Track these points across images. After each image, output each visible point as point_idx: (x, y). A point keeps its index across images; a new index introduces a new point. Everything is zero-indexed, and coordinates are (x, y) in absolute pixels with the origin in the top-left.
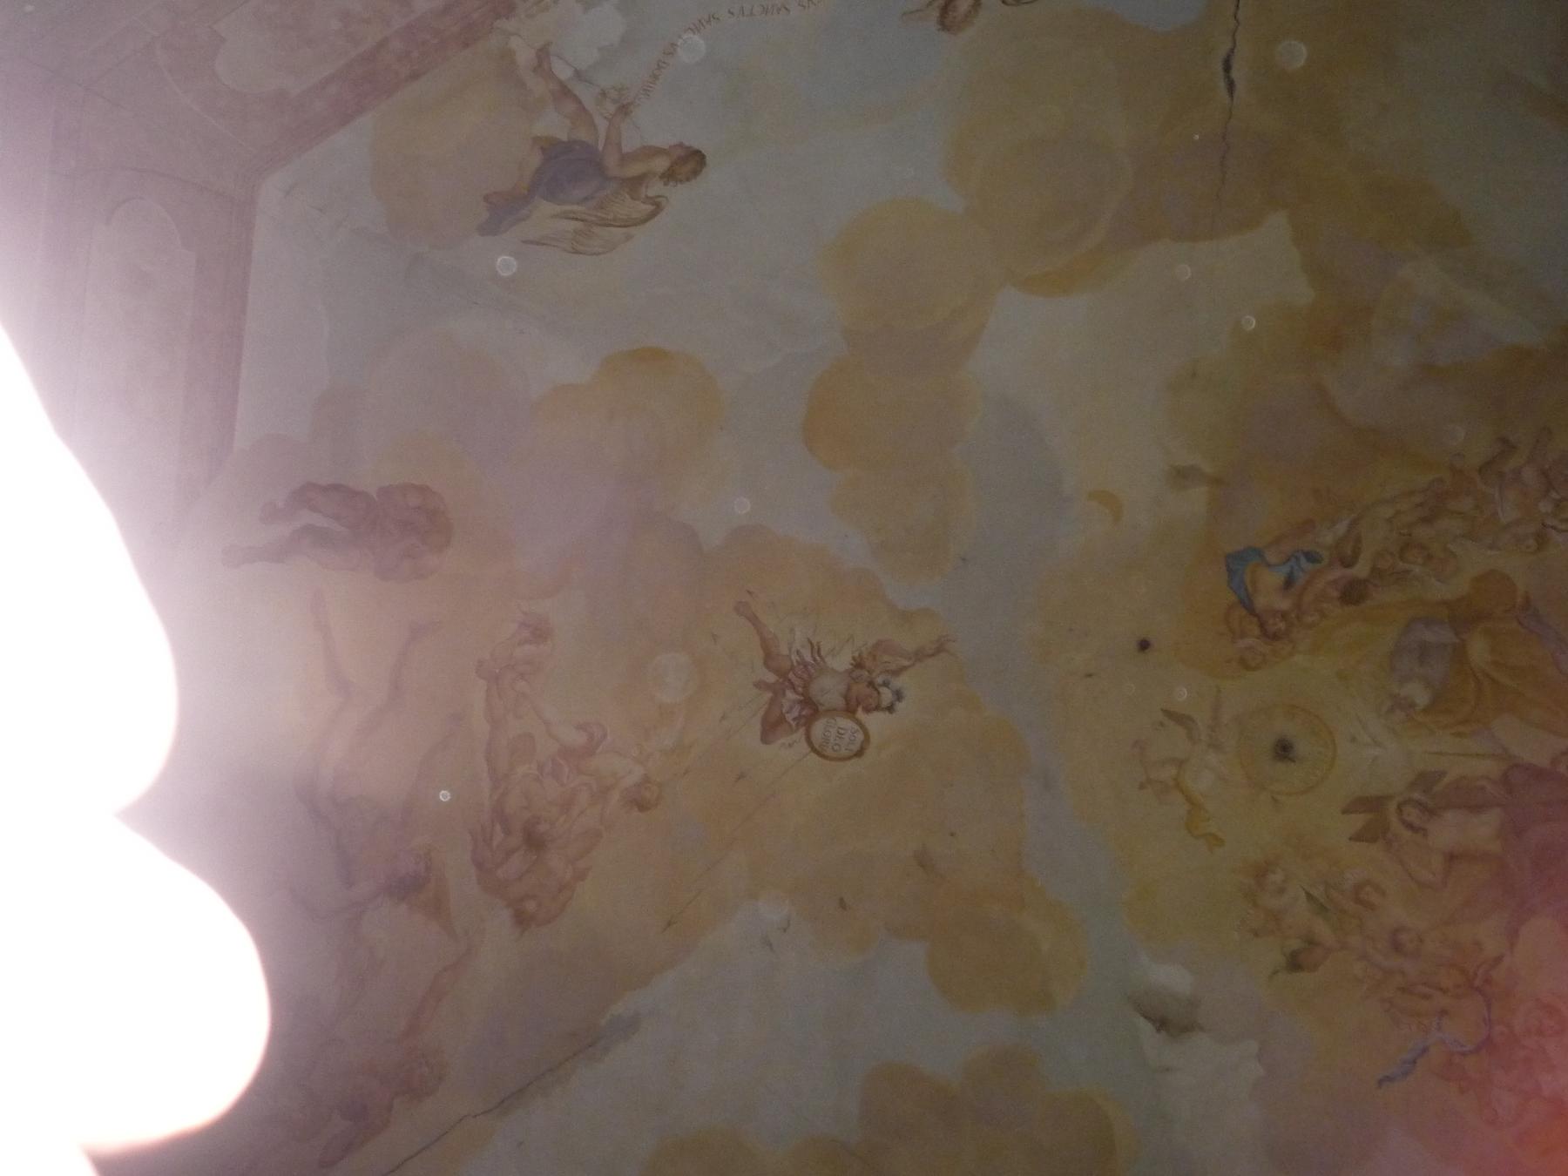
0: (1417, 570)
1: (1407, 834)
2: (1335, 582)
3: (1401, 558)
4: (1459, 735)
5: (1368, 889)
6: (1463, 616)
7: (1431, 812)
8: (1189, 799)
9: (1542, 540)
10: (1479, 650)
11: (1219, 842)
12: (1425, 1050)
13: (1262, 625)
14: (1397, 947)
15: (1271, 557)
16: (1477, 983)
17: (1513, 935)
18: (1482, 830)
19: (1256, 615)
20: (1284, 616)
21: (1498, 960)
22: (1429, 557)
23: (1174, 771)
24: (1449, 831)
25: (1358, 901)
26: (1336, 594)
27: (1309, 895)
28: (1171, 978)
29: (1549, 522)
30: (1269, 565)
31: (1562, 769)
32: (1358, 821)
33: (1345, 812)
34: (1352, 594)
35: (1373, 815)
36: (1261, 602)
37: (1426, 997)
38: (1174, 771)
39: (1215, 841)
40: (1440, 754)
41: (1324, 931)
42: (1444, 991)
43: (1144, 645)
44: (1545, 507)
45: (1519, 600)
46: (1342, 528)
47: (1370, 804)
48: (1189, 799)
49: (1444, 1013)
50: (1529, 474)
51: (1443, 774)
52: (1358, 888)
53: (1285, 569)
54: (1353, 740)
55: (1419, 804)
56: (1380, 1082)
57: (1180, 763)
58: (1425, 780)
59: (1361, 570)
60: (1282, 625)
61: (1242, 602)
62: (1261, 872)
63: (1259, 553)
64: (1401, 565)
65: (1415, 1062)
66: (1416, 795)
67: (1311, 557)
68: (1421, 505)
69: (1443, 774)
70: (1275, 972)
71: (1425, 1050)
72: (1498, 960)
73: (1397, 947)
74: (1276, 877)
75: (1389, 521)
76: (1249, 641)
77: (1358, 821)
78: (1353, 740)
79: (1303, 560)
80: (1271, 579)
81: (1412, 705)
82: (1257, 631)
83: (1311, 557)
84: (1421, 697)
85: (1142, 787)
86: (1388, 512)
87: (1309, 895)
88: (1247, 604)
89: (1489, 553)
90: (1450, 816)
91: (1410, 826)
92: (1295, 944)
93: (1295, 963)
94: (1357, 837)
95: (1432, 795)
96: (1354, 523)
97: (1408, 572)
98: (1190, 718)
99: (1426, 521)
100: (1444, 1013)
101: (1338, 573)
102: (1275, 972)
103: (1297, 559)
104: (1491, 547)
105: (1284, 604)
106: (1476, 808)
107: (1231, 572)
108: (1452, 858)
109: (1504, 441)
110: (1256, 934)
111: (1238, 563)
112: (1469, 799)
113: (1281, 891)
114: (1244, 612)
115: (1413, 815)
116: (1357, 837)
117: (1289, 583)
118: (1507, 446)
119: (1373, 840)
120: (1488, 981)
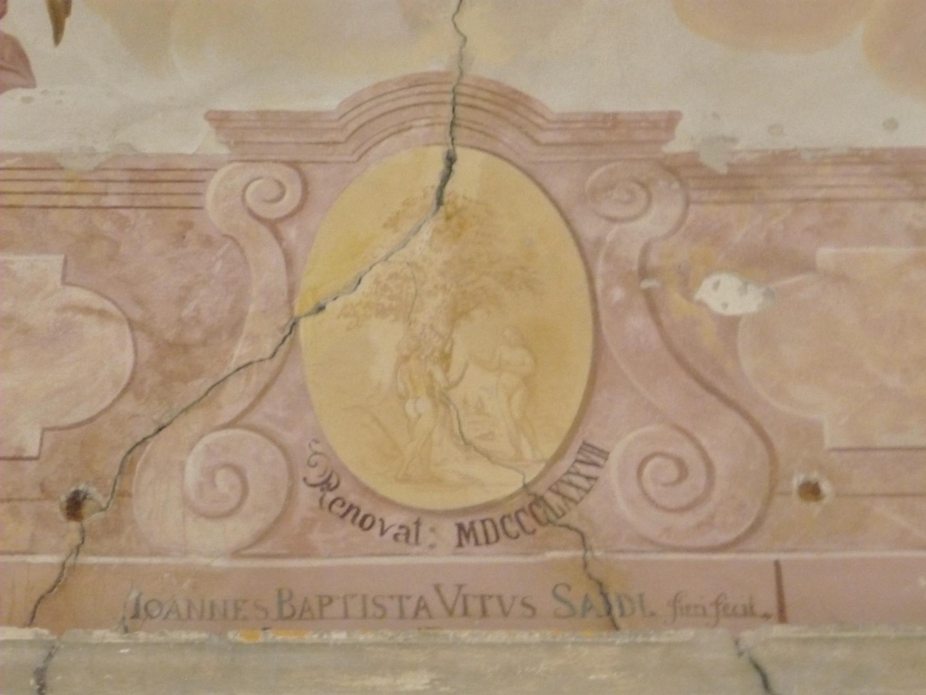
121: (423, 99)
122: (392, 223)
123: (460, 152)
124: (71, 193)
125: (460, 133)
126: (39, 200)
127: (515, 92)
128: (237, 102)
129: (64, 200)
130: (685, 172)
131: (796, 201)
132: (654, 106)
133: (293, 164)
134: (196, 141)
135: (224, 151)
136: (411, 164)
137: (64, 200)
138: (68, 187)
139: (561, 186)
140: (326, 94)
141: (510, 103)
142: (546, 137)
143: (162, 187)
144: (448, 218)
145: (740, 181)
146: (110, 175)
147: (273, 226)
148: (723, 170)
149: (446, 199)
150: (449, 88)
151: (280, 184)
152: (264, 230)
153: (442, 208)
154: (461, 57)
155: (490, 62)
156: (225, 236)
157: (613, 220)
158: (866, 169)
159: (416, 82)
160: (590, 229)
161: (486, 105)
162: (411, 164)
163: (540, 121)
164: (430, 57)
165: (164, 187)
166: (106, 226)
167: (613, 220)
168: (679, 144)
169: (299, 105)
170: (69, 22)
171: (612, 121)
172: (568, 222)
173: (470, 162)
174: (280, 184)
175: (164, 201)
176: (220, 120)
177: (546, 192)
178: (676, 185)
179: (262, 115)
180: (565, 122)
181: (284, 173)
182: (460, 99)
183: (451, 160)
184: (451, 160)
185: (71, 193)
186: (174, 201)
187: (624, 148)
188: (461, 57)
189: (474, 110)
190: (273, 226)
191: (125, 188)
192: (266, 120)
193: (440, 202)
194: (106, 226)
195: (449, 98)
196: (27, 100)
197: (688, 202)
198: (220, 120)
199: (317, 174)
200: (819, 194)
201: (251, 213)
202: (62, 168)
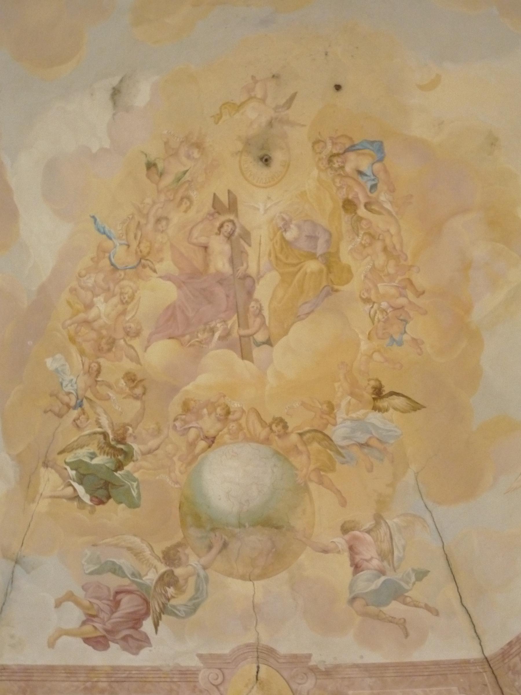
0: (359, 240)
1: (218, 224)
2: (358, 198)
3: (365, 234)
4: (270, 255)
5: (188, 203)
6: (330, 260)
7: (229, 237)
8: (242, 104)
9: (367, 301)
10: (312, 266)
11: (217, 123)
12: (110, 238)
13: (338, 155)
14: (158, 220)
15: (377, 166)
16: (143, 261)
17: (168, 277)
18: (220, 264)
19: (345, 152)
20: (342, 168)
21: (155, 271)
22: (364, 247)
23: (259, 96)
24: (219, 247)
25: (182, 199)
26: (350, 197)
27: (185, 173)
28: (142, 94)
29: (376, 306)
30: (373, 164)
31: (253, 304)
32: (224, 198)
33: (229, 192)
34: (349, 205)
35: (226, 207)
36: (352, 156)
37: (135, 237)
38: (259, 96)
39: (218, 118)
40: (260, 244)
41: (168, 180)
42: (138, 246)
43: (338, 87)
44: (384, 305)
45: (336, 287)
46: (388, 206)
47: (233, 206)
48: (242, 104)
49: (128, 246)
50: (402, 301)
51: (250, 245)
52: (189, 198)
53: (369, 173)
54: (269, 198)
55: (234, 231)
56: (93, 217)
57: (263, 100)
58: (246, 235)
59: (362, 211)
60: (336, 165)
61: (354, 146)
62: (198, 145)
63: (381, 160)
64: (361, 232)
65: (104, 233)
66: (238, 231)
67: (374, 187)
68: (394, 247)
69: (250, 245)
70: (146, 155)
71: (110, 238)
72: (155, 271)
73: (158, 220)
74: (196, 154)
75: (388, 231)
76: (329, 146)
77: (224, 198)
78: (269, 198)
79: (373, 183)
80: (365, 164)
81: (285, 231)
82: (335, 151)
83: (374, 187)
84: (290, 235)
85: (253, 77)
86: (393, 231)
87: (185, 173)
88: (352, 148)
89: (362, 276)
90: (227, 247)
91: (222, 226)
92: (160, 166)
93: (150, 166)
94: (215, 197)
95: (238, 240)
96: (389, 213)
97: (358, 235)
98: (289, 108)
99: (385, 249)
100: (128, 246)
101: (362, 199)
102: (146, 155)
103: (373, 180)
104: (365, 277)
105: (349, 168)
106: (232, 261)
107: (372, 143)
108: (206, 248)
109: (423, 293)
110: (166, 143)
111: (378, 149)
112: (236, 257)
113: (189, 157)
114: (347, 146)
115: (228, 228)
116: (215, 197)
117: (360, 173)
118: (420, 294)
119: (214, 206)
120: (144, 266)
121: (250, 650)
122: (247, 685)
123: (261, 665)
124: (164, 678)
125: (260, 660)
126: (158, 680)
127: (271, 648)
128: (204, 651)
129: (163, 680)
130: (314, 670)
131: (342, 678)
132: (306, 652)
133: (220, 669)
134: (194, 662)
135: (202, 665)
136: (248, 668)
137: (163, 680)
138: (163, 676)
139: (286, 674)
140: (226, 649)
141: (271, 651)
142: (281, 661)
143: (187, 675)
144: (260, 684)
145: (328, 673)
146: (174, 672)
147: (217, 686)
148: (324, 670)
149: (259, 678)
150: (255, 647)
151: (217, 675)
152: (215, 688)
153: (258, 682)
154: (258, 639)
155: (265, 640)
156: (206, 690)
157: (299, 684)
158: (357, 669)
159: (247, 645)
160: (294, 686)
161: (265, 652)
162: (248, 668)
163: (278, 656)
164: (250, 638)
165: (189, 676)
166: (174, 687)
167: (299, 684)
168: (312, 663)
169: (219, 652)
170: (159, 628)
171: (295, 656)
172: (288, 685)
173: (263, 668)
174: (217, 675)
175: (189, 679)
176: (200, 656)
177: (282, 676)
178: (313, 674)
179: (210, 655)
180: (285, 656)
181: (218, 671)
182: (259, 650)
183: (258, 667)
184: (258, 667)
185: (164, 678)
186: (192, 680)
187: (297, 661)
188: (258, 639)
189: (264, 653)
190: (217, 686)
191: (178, 676)
192: (212, 656)
193: (257, 679)
194: (174, 687)
195: (256, 650)
196: (150, 651)
197: (316, 679)
198: (200, 656)
199: (226, 672)
200: (347, 676)
201: (211, 683)
202: (161, 670)
